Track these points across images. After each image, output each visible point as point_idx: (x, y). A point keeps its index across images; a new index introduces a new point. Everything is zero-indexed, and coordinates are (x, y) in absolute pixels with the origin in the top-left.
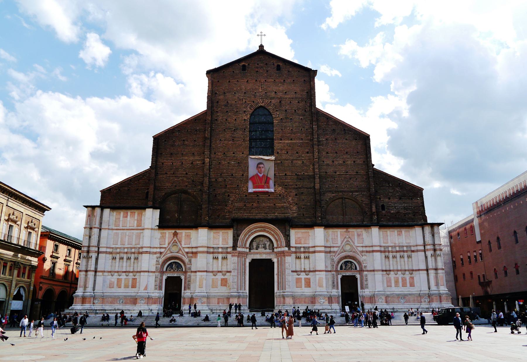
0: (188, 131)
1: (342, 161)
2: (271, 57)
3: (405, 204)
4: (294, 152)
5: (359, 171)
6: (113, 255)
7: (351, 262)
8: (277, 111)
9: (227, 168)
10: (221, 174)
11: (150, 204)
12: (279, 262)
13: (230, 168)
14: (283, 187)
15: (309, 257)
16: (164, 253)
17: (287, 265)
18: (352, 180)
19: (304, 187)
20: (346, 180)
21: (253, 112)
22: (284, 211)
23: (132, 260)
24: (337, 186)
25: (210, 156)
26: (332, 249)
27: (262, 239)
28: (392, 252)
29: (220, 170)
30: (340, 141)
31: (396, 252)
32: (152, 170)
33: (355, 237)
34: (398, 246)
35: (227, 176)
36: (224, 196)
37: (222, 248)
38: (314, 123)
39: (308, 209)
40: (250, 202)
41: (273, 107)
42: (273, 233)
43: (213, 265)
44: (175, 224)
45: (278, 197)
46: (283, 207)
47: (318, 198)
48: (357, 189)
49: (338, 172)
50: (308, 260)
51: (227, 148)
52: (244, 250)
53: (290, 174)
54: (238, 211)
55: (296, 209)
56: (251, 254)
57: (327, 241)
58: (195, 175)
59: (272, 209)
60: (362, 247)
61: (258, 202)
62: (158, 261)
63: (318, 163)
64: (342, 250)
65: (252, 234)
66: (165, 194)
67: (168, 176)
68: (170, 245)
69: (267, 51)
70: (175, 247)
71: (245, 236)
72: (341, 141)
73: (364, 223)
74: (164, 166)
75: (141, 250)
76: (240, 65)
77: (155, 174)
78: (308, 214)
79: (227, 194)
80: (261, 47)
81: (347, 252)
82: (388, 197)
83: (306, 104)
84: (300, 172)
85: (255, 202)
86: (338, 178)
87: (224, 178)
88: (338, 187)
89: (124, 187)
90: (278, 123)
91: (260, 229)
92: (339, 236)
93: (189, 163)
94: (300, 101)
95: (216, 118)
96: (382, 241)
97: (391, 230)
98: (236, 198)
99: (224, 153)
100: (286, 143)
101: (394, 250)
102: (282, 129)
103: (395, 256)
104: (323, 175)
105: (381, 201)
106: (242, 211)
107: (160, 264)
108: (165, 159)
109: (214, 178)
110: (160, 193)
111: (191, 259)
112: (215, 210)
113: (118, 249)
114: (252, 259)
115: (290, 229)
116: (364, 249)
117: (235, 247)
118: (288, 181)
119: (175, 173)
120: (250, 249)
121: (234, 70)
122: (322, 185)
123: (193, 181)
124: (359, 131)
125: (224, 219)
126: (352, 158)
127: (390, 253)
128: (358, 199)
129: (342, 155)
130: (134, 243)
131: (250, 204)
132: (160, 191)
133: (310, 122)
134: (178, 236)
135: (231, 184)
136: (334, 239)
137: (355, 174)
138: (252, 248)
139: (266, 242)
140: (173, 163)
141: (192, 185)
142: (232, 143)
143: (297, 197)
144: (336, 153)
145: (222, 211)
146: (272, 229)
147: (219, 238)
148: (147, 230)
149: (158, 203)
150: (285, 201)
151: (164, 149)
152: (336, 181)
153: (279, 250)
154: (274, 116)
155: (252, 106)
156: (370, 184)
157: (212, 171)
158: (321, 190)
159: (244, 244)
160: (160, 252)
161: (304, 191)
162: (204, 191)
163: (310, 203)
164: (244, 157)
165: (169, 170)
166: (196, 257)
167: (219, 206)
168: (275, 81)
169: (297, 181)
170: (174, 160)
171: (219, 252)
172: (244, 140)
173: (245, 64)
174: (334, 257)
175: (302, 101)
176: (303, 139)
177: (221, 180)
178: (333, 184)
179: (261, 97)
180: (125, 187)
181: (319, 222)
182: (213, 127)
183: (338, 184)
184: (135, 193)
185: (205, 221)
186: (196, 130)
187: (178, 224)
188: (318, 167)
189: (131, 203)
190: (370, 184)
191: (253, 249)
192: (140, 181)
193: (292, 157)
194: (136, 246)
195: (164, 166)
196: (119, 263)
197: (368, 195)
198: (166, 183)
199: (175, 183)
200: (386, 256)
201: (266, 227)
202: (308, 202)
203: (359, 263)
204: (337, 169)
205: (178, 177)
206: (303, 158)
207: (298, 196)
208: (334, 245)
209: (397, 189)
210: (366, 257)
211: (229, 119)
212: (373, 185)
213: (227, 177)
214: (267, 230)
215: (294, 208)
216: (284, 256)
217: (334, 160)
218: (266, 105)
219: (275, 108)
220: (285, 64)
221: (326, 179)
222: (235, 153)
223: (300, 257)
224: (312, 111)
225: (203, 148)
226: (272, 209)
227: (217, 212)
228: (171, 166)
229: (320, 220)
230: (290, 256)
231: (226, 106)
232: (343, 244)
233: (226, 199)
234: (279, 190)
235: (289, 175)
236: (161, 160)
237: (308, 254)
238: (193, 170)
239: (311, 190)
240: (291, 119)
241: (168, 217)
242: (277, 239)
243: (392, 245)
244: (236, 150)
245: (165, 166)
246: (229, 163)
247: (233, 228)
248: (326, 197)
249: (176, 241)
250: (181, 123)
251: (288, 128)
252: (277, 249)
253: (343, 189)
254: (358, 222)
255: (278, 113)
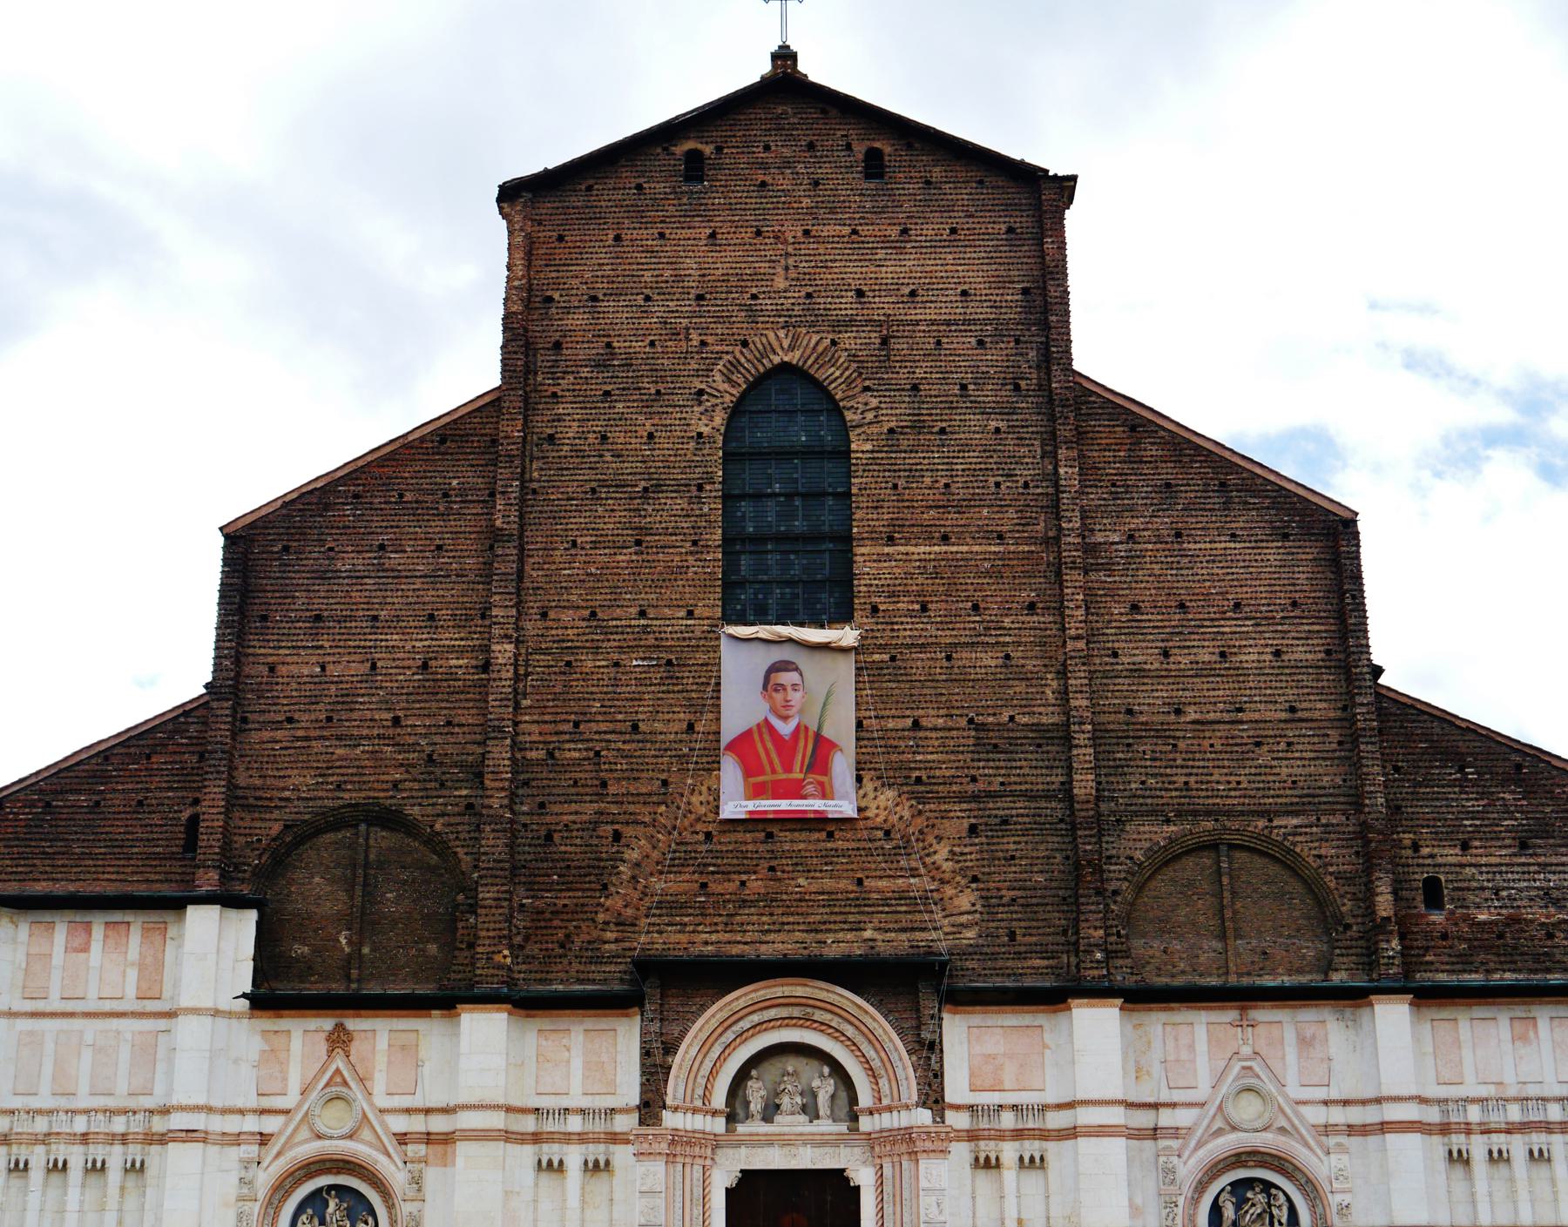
0: (401, 496)
1: (1211, 650)
2: (833, 112)
3: (1551, 876)
4: (961, 605)
5: (1304, 705)
6: (15, 1148)
7: (1267, 1186)
8: (867, 389)
9: (610, 689)
10: (576, 724)
11: (208, 880)
12: (888, 1188)
13: (624, 689)
14: (905, 789)
15: (1042, 1159)
16: (283, 1140)
17: (926, 1201)
18: (1266, 748)
19: (1018, 787)
20: (1236, 748)
21: (744, 395)
22: (909, 917)
23: (114, 1174)
24: (1186, 783)
25: (518, 628)
26: (1166, 1118)
27: (792, 1063)
28: (1482, 1133)
29: (572, 703)
30: (1203, 546)
31: (1508, 1132)
32: (215, 705)
33: (1287, 1049)
34: (1516, 1099)
35: (605, 732)
36: (595, 841)
37: (582, 1111)
38: (1062, 453)
39: (1037, 905)
40: (730, 869)
41: (847, 369)
42: (850, 1031)
43: (535, 1201)
44: (337, 988)
45: (878, 844)
46: (902, 895)
47: (1089, 847)
48: (1297, 800)
49: (1191, 709)
50: (1039, 1171)
51: (606, 584)
52: (698, 1122)
53: (941, 721)
54: (666, 919)
55: (974, 905)
56: (738, 1145)
57: (1140, 1073)
58: (441, 730)
59: (847, 909)
60: (1326, 1103)
61: (772, 869)
62: (250, 1182)
63: (1084, 664)
64: (1219, 1124)
65: (743, 1037)
66: (286, 827)
67: (300, 733)
68: (314, 1095)
69: (813, 78)
70: (339, 1104)
71: (705, 1047)
72: (1208, 546)
73: (1337, 978)
74: (277, 684)
75: (159, 1124)
76: (673, 154)
77: (233, 724)
78: (1034, 931)
79: (609, 828)
80: (784, 57)
81: (1246, 1131)
82: (1460, 836)
83: (1022, 355)
84: (991, 711)
85: (755, 873)
86: (1195, 742)
87: (591, 745)
88: (1195, 786)
89: (71, 791)
90: (872, 452)
91: (784, 1012)
92: (1202, 1046)
93: (409, 668)
94: (988, 340)
95: (549, 431)
96: (1431, 1075)
97: (1479, 1011)
98: (654, 847)
99: (593, 614)
100: (916, 557)
101: (1496, 1118)
102: (895, 486)
103: (1500, 1152)
104: (1111, 727)
105: (1421, 861)
106: (686, 919)
107: (262, 1193)
108: (283, 644)
109: (540, 742)
110: (258, 824)
111: (421, 1171)
112: (548, 916)
113: (38, 1119)
114: (742, 1171)
115: (940, 1011)
116: (1338, 1116)
117: (650, 1107)
118: (930, 757)
119: (336, 717)
120: (731, 1118)
121: (641, 180)
122: (1112, 779)
123: (430, 759)
124: (1301, 492)
125: (591, 963)
126: (1267, 635)
127: (1473, 1137)
128: (1298, 850)
129: (1212, 620)
130: (122, 1087)
131: (729, 880)
132: (257, 815)
133: (1042, 446)
134: (354, 1048)
135: (626, 774)
136: (1177, 1061)
137: (1281, 721)
138: (741, 1113)
139: (816, 1083)
140: (323, 668)
141: (425, 780)
142: (634, 557)
143: (977, 841)
144: (1182, 606)
145: (581, 916)
146: (843, 1013)
147: (568, 1062)
148: (190, 1016)
149: (247, 875)
150: (914, 864)
151: (277, 595)
152: (1184, 756)
153: (886, 1121)
154: (855, 417)
155: (735, 365)
156: (1365, 770)
157: (530, 707)
158: (1103, 807)
159: (700, 1091)
160: (261, 1134)
161: (1014, 812)
162: (491, 812)
163: (1048, 876)
164: (698, 634)
165: (307, 700)
166: (446, 1161)
167: (569, 890)
168: (855, 232)
169: (976, 756)
170: (329, 651)
171: (570, 1134)
172: (695, 543)
173: (699, 146)
174: (1175, 1160)
175: (999, 335)
176: (1008, 535)
177: (577, 755)
178: (1168, 771)
179: (782, 319)
180: (78, 792)
181: (1096, 973)
182: (536, 474)
183: (1195, 771)
184: (130, 822)
185: (496, 972)
186: (446, 495)
187: (354, 986)
188: (1087, 681)
189: (106, 876)
190: (1365, 770)
191: (748, 1116)
192: (153, 760)
193: (948, 633)
194: (132, 1103)
195: (280, 680)
196: (44, 1194)
197: (1351, 829)
198: (289, 772)
199: (338, 771)
200: (1455, 1154)
201: (818, 1004)
202: (1035, 869)
203: (1310, 1188)
204: (1187, 694)
205: (355, 742)
206: (1007, 639)
207: (984, 840)
208: (1177, 1096)
209: (1507, 796)
210: (1345, 1158)
211: (618, 437)
212: (1376, 773)
213: (608, 737)
214: (819, 1015)
215: (965, 901)
216: (913, 1155)
217: (1171, 644)
218: (810, 362)
219: (861, 374)
220: (910, 146)
221: (1129, 745)
222: (651, 613)
223: (997, 1159)
224: (1051, 390)
225: (481, 586)
226: (847, 909)
227: (556, 923)
228: (317, 680)
229: (1098, 962)
230: (942, 1155)
231: (600, 365)
232: (1224, 1090)
233: (604, 855)
234: (882, 805)
235: (935, 729)
236: (262, 651)
237: (1037, 1143)
238: (427, 705)
239: (1054, 804)
240: (943, 431)
241: (301, 950)
242: (876, 1064)
243: (1483, 1092)
244: (653, 596)
245: (286, 680)
246: (617, 664)
247: (641, 1006)
248: (1131, 843)
249: (342, 1076)
250: (369, 458)
251: (928, 480)
252: (876, 1116)
253: (1218, 801)
254: (1300, 971)
255: (874, 402)
